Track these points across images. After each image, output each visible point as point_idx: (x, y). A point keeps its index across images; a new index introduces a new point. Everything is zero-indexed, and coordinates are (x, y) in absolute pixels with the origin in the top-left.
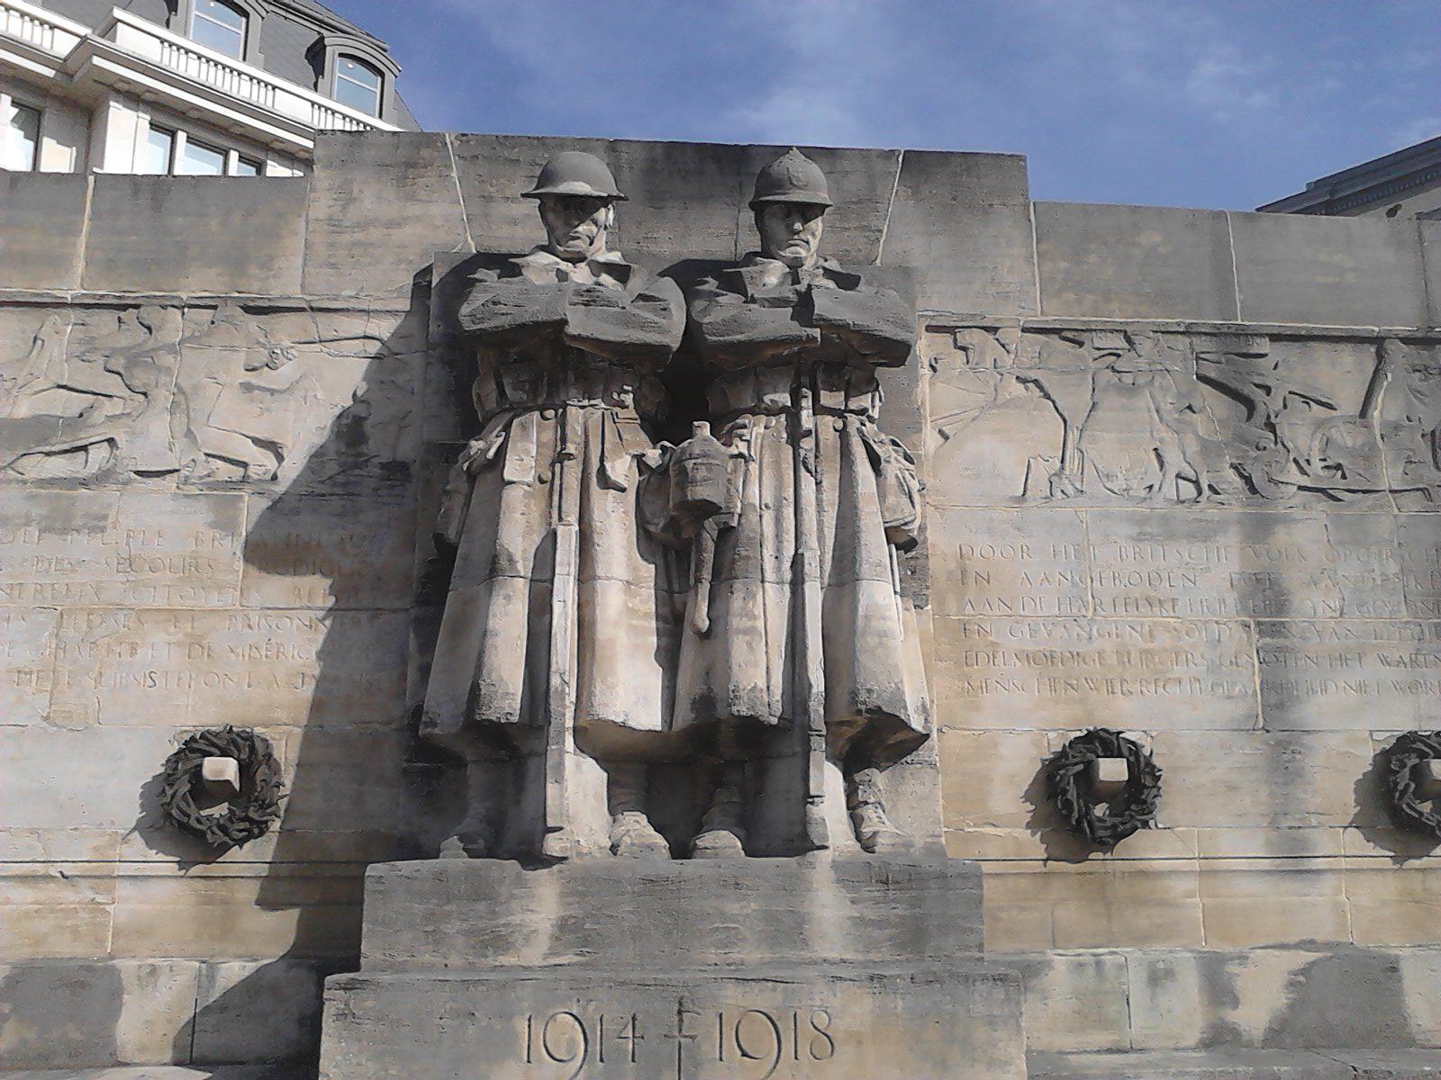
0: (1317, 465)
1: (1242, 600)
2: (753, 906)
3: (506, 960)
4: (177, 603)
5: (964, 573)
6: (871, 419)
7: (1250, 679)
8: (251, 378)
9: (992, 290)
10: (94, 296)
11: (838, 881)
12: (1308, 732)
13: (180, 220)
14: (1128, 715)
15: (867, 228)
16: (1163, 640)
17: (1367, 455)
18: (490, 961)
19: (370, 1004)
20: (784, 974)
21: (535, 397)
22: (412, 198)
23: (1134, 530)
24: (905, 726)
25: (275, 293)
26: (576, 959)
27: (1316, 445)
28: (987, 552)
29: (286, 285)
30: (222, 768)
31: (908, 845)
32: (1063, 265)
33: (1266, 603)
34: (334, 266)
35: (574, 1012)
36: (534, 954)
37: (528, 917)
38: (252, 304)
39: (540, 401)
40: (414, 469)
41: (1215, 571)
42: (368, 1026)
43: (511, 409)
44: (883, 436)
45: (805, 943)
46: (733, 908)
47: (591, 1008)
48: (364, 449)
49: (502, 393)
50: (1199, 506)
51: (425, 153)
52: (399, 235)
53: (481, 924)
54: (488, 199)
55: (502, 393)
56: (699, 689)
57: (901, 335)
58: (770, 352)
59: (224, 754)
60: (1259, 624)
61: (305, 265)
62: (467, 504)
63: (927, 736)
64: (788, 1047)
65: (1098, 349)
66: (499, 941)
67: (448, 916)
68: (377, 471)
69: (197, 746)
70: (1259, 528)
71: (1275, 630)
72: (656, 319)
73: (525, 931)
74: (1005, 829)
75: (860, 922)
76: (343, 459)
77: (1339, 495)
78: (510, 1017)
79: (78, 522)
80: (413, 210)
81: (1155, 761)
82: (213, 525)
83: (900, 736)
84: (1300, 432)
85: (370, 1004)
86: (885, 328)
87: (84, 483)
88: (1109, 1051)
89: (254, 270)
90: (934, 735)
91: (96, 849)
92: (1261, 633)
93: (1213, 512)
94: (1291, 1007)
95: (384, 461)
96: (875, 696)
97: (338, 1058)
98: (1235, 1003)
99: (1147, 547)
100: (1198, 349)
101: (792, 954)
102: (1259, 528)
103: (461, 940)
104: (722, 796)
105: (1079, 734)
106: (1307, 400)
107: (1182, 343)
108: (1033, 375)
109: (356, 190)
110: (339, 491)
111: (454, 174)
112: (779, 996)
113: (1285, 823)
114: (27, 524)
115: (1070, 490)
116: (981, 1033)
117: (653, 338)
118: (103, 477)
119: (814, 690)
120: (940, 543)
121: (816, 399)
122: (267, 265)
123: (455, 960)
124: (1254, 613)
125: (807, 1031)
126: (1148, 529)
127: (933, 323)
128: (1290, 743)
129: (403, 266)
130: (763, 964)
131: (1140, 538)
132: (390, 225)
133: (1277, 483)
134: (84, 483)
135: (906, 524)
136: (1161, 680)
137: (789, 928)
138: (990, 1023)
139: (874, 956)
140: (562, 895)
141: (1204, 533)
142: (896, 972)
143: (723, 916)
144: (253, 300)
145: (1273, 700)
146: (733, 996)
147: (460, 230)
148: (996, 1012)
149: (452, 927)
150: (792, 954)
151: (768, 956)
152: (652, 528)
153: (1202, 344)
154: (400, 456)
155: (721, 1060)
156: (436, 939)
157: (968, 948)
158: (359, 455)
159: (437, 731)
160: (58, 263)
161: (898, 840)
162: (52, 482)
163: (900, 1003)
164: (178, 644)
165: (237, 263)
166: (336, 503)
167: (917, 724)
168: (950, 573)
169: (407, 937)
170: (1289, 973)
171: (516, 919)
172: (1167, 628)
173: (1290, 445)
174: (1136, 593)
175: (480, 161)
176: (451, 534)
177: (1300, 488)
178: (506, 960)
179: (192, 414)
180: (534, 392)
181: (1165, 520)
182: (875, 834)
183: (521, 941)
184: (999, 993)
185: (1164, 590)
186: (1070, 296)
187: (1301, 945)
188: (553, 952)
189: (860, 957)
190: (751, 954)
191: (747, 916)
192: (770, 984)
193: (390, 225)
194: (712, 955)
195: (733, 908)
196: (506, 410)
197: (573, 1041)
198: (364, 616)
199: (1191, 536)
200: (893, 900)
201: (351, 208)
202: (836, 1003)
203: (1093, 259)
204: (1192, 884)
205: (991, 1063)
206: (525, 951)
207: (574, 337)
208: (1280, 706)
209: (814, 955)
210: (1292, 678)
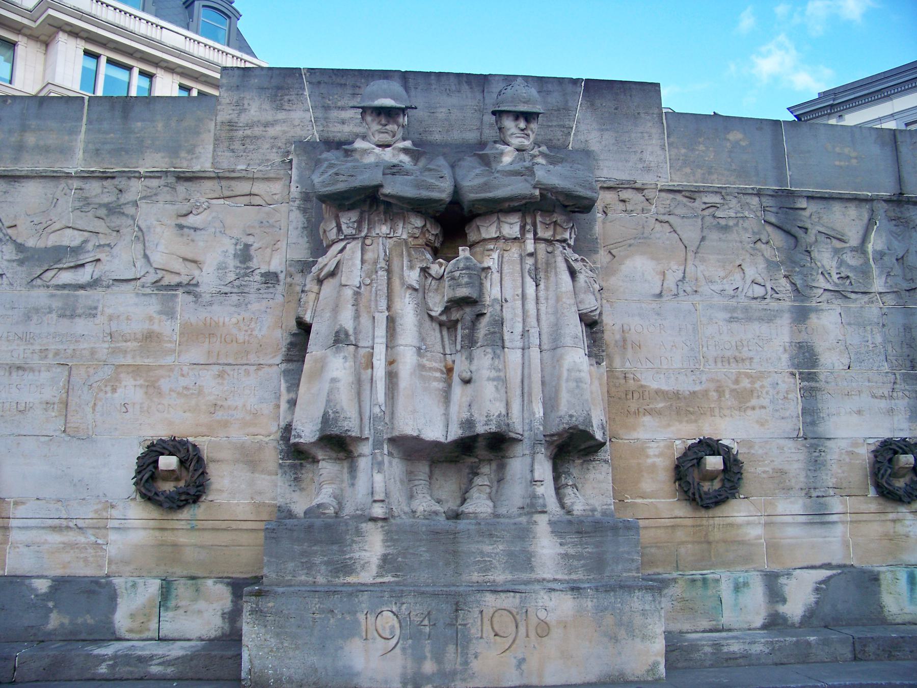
0: (835, 277)
1: (792, 358)
2: (501, 547)
3: (351, 579)
4: (139, 362)
5: (625, 340)
6: (569, 246)
7: (795, 406)
8: (182, 221)
9: (641, 166)
10: (88, 172)
11: (552, 532)
12: (829, 439)
13: (139, 124)
14: (728, 430)
16: (745, 383)
17: (864, 272)
18: (341, 580)
19: (271, 604)
20: (522, 588)
21: (360, 231)
22: (280, 108)
23: (728, 316)
24: (592, 437)
25: (196, 168)
26: (392, 579)
27: (834, 264)
28: (639, 329)
29: (203, 163)
30: (168, 462)
31: (593, 510)
32: (683, 151)
33: (806, 363)
34: (233, 151)
35: (394, 610)
36: (366, 576)
37: (363, 553)
38: (182, 175)
39: (363, 234)
40: (282, 277)
41: (775, 341)
42: (270, 618)
43: (346, 238)
44: (577, 256)
45: (532, 569)
46: (488, 548)
47: (404, 607)
48: (250, 264)
49: (339, 229)
50: (766, 301)
51: (289, 81)
52: (272, 131)
53: (336, 558)
54: (327, 108)
55: (339, 229)
56: (465, 415)
57: (589, 194)
58: (507, 205)
59: (171, 454)
60: (800, 373)
61: (214, 151)
62: (317, 299)
63: (604, 444)
64: (522, 630)
65: (705, 203)
66: (347, 568)
67: (315, 553)
68: (258, 278)
69: (154, 450)
70: (801, 315)
71: (810, 377)
72: (437, 183)
73: (362, 562)
74: (657, 501)
75: (566, 556)
76: (238, 271)
77: (849, 295)
78: (355, 613)
79: (80, 311)
80: (281, 115)
81: (740, 457)
82: (160, 313)
83: (592, 443)
84: (825, 258)
85: (271, 604)
86: (580, 189)
87: (82, 287)
88: (711, 631)
89: (183, 154)
90: (608, 443)
91: (96, 511)
92: (802, 379)
93: (774, 305)
95: (263, 271)
96: (574, 419)
97: (253, 636)
98: (784, 601)
99: (735, 326)
100: (764, 204)
101: (525, 576)
102: (801, 315)
103: (323, 568)
104: (478, 481)
105: (694, 441)
106: (829, 237)
107: (755, 201)
108: (666, 218)
109: (246, 102)
110: (236, 290)
111: (307, 93)
112: (517, 601)
113: (814, 494)
114: (50, 312)
115: (688, 289)
116: (638, 620)
117: (435, 195)
118: (94, 284)
119: (537, 416)
120: (611, 322)
121: (535, 234)
122: (191, 151)
123: (321, 579)
124: (797, 366)
125: (533, 621)
126: (735, 315)
127: (605, 185)
128: (818, 445)
129: (274, 150)
130: (506, 582)
131: (731, 320)
132: (267, 125)
133: (812, 287)
134: (82, 287)
135: (591, 312)
138: (644, 615)
139: (574, 577)
140: (384, 541)
141: (769, 318)
142: (586, 585)
143: (482, 553)
144: (184, 172)
146: (490, 600)
147: (310, 128)
148: (647, 607)
149: (318, 560)
150: (525, 576)
151: (510, 577)
152: (433, 314)
153: (767, 202)
154: (273, 268)
155: (481, 638)
156: (309, 567)
157: (630, 570)
158: (248, 268)
159: (302, 440)
160: (65, 151)
161: (587, 507)
162: (64, 287)
163: (590, 604)
164: (141, 386)
165: (173, 151)
166: (234, 298)
167: (599, 436)
168: (616, 341)
169: (291, 565)
171: (356, 555)
172: (748, 375)
173: (819, 264)
174: (728, 354)
175: (322, 85)
176: (308, 318)
178: (351, 579)
179: (147, 244)
180: (359, 229)
181: (746, 309)
182: (573, 504)
183: (359, 569)
184: (648, 597)
185: (745, 353)
186: (688, 170)
187: (821, 567)
188: (379, 575)
189: (566, 577)
190: (500, 576)
191: (497, 554)
192: (512, 594)
193: (267, 125)
194: (475, 577)
195: (488, 548)
196: (342, 240)
197: (393, 627)
198: (253, 368)
199: (761, 319)
200: (587, 543)
201: (243, 115)
202: (551, 604)
203: (702, 147)
205: (644, 638)
206: (363, 574)
207: (386, 196)
208: (813, 423)
209: (538, 577)
210: (820, 406)
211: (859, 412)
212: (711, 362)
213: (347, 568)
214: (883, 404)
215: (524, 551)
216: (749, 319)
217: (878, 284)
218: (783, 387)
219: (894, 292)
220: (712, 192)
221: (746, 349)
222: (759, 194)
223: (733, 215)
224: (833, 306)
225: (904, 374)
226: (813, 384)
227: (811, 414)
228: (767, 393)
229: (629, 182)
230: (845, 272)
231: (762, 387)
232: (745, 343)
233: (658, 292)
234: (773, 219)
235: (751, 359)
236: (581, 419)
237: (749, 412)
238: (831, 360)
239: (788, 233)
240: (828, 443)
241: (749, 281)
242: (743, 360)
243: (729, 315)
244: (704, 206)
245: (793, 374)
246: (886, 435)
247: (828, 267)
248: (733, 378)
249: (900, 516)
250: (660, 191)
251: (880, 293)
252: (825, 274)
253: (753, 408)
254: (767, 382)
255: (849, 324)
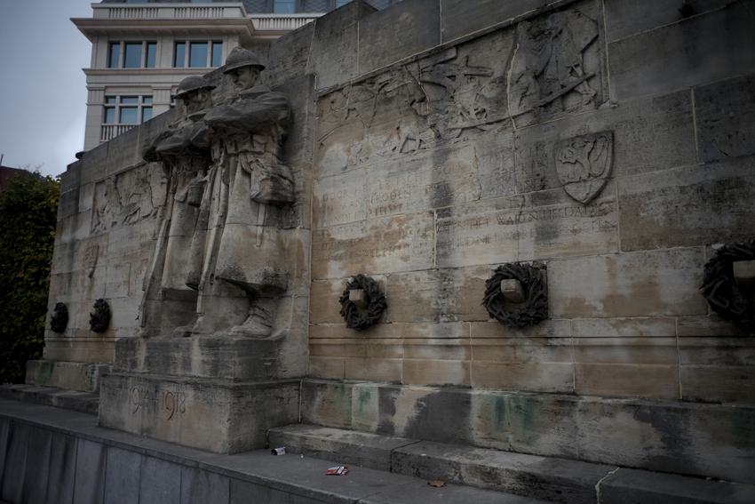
1: (432, 199)
12: (456, 269)
15: (302, 61)
16: (395, 226)
32: (368, 46)
33: (442, 200)
60: (437, 211)
70: (442, 155)
75: (203, 361)
93: (421, 155)
94: (419, 418)
98: (393, 412)
100: (421, 67)
126: (392, 171)
128: (448, 275)
135: (258, 195)
136: (392, 248)
137: (187, 364)
145: (441, 251)
149: (128, 359)
170: (418, 400)
172: (398, 220)
173: (459, 106)
174: (386, 204)
177: (463, 129)
185: (398, 201)
188: (144, 369)
195: (176, 355)
199: (409, 170)
203: (380, 38)
204: (400, 351)
211: (486, 240)
212: (374, 214)
213: (134, 364)
214: (511, 229)
215: (189, 358)
216: (402, 171)
217: (513, 108)
218: (423, 225)
219: (529, 112)
220: (385, 73)
221: (398, 197)
222: (417, 60)
223: (396, 86)
224: (469, 142)
225: (532, 195)
226: (447, 219)
227: (443, 248)
228: (411, 233)
229: (334, 87)
230: (481, 106)
231: (408, 228)
232: (397, 193)
233: (344, 165)
234: (427, 78)
235: (401, 205)
236: (222, 272)
237: (396, 251)
238: (463, 194)
239: (439, 85)
240: (456, 272)
241: (403, 140)
242: (395, 207)
243: (387, 172)
244: (380, 86)
245: (432, 213)
246: (511, 260)
247: (467, 106)
248: (387, 223)
249: (518, 342)
250: (353, 85)
251: (514, 117)
252: (465, 111)
253: (399, 247)
254: (411, 223)
255: (483, 156)
